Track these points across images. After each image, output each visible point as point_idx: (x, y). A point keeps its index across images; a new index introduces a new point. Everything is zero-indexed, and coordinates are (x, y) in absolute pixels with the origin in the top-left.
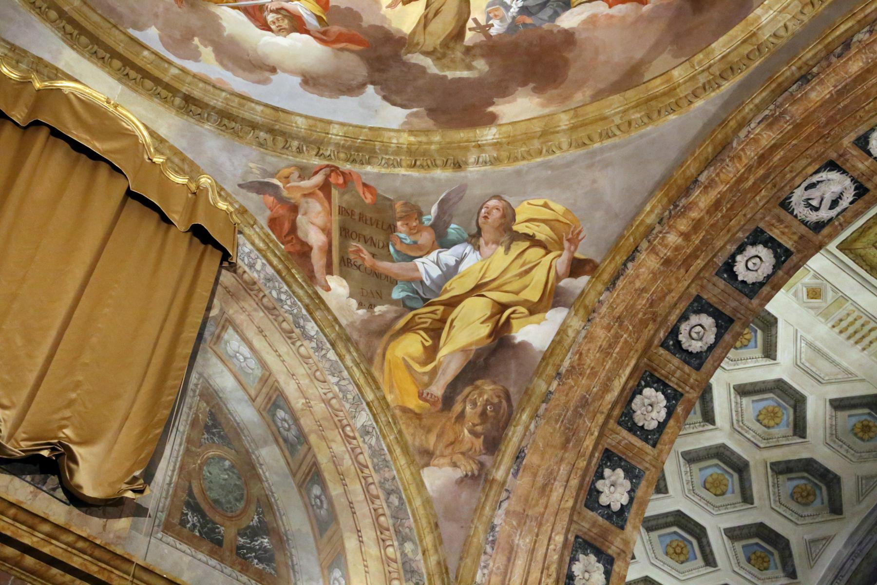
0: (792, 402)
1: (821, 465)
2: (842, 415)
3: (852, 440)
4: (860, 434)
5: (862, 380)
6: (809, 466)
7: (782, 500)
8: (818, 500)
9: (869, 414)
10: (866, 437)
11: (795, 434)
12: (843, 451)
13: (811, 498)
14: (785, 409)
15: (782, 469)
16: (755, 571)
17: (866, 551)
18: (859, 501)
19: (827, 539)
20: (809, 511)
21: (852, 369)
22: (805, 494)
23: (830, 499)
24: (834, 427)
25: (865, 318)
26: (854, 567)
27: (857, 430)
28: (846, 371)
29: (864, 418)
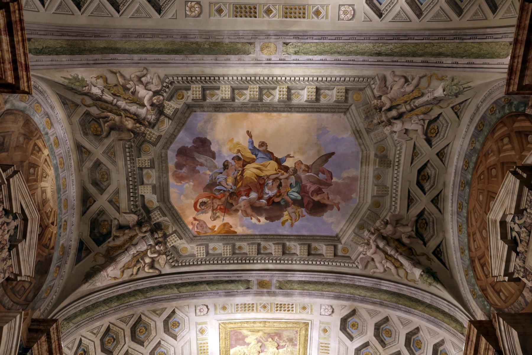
0: (359, 352)
1: (375, 332)
2: (353, 335)
3: (360, 327)
4: (357, 326)
5: (339, 337)
6: (377, 334)
7: (394, 340)
8: (387, 327)
9: (348, 328)
10: (356, 324)
11: (369, 345)
12: (365, 328)
13: (387, 330)
14: (362, 353)
15: (383, 344)
16: (423, 345)
17: (395, 304)
18: (380, 312)
19: (399, 318)
20: (392, 329)
21: (337, 342)
22: (387, 333)
23: (384, 323)
24: (359, 335)
25: (320, 351)
26: (404, 307)
27: (356, 328)
28: (339, 343)
29: (351, 329)
